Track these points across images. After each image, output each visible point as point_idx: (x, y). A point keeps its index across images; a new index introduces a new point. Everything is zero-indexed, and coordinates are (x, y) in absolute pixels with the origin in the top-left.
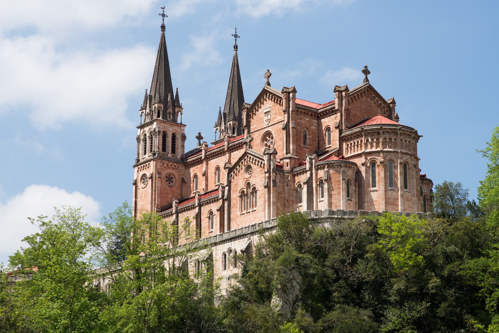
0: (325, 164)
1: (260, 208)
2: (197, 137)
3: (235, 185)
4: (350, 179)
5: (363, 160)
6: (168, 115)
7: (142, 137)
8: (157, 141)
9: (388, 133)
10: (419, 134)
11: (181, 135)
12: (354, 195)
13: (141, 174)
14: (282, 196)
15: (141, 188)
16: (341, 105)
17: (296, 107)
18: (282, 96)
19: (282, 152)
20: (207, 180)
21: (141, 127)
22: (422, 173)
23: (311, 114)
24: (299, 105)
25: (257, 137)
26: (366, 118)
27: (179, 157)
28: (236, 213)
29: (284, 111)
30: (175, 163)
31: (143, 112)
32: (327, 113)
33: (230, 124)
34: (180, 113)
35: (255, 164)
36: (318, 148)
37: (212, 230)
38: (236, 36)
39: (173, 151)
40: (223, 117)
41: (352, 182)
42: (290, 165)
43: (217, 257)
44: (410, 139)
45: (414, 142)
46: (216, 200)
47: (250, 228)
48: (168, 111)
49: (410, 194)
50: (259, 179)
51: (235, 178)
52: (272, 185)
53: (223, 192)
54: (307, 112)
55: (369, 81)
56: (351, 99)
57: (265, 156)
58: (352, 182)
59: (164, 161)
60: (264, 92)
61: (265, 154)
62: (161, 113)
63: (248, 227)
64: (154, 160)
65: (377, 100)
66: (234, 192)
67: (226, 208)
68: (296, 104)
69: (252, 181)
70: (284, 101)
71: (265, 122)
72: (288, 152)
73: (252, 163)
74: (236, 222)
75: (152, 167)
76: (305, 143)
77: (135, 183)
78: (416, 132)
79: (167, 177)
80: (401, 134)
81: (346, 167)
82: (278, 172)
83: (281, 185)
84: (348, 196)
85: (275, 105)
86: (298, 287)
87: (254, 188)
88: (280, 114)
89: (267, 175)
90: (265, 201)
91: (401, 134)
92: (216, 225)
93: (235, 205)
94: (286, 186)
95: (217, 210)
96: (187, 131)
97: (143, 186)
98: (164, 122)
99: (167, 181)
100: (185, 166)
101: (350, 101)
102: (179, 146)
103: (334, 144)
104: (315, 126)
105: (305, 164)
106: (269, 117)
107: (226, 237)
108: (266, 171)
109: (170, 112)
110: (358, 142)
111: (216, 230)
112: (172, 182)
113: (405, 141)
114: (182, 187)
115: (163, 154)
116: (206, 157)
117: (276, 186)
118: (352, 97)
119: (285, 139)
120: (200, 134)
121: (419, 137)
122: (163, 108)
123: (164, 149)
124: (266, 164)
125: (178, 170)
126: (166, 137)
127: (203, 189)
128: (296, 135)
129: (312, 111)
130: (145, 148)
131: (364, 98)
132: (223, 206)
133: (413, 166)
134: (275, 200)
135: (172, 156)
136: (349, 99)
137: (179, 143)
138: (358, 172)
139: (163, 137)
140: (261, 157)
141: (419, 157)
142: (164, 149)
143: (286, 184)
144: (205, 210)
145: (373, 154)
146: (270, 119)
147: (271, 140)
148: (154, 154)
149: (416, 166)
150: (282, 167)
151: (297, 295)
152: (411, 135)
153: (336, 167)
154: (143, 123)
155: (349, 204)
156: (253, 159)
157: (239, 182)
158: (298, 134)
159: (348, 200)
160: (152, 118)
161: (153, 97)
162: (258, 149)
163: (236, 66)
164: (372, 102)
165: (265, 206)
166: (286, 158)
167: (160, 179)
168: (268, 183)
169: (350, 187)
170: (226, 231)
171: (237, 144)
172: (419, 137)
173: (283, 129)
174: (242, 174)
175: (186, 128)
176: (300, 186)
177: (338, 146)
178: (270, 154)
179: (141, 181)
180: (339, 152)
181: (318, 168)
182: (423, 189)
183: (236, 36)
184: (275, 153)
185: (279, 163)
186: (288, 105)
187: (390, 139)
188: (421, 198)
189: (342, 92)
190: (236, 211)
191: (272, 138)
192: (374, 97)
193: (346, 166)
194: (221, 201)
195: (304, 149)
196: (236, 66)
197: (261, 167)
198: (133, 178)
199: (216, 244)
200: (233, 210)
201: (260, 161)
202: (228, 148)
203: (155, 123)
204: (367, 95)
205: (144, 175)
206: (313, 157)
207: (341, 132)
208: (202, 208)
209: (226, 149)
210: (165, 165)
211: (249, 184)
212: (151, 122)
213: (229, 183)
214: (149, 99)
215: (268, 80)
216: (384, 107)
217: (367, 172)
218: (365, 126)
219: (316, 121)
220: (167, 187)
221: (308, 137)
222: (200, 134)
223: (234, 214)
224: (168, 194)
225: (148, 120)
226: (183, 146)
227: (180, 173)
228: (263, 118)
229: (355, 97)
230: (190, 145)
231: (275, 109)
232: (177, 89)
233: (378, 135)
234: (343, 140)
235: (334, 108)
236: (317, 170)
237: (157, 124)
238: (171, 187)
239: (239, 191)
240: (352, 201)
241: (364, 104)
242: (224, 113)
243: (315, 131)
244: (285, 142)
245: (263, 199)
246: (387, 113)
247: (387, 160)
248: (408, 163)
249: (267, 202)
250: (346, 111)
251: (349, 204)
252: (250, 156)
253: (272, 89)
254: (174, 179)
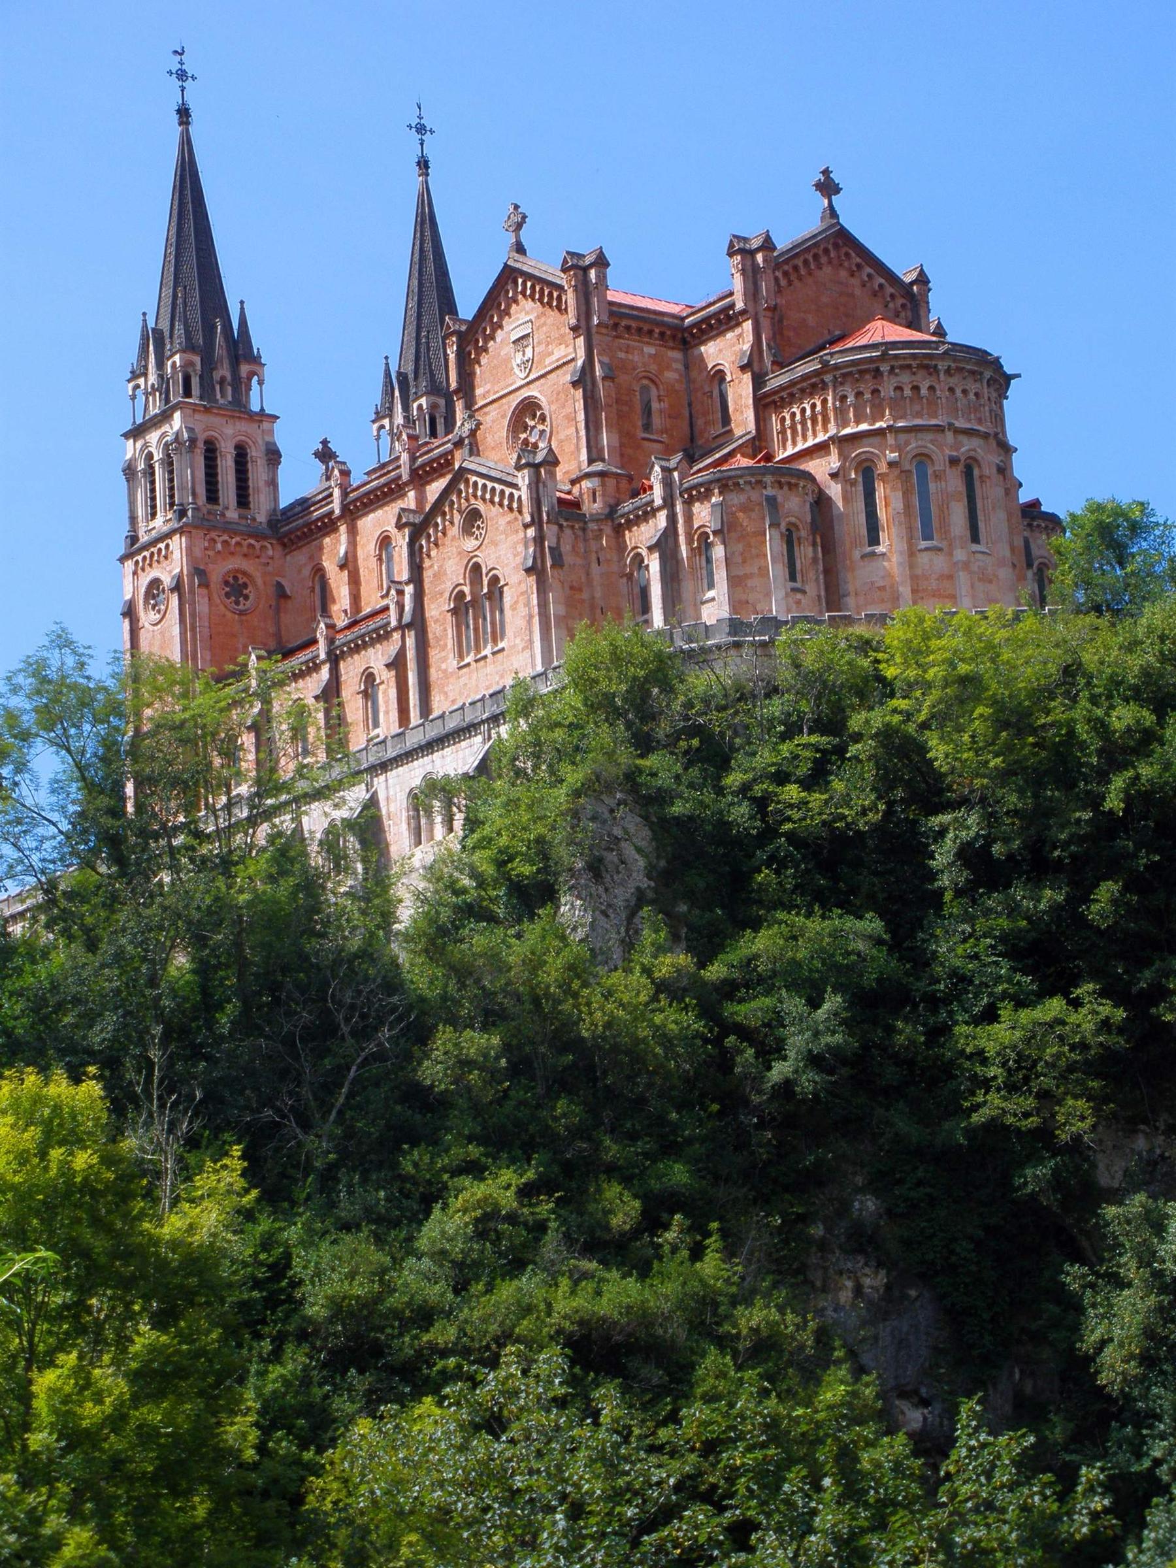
0: (711, 482)
1: (518, 641)
2: (317, 454)
3: (435, 575)
4: (794, 524)
5: (833, 461)
6: (218, 387)
7: (141, 466)
8: (191, 473)
9: (908, 372)
10: (1008, 370)
11: (263, 448)
12: (812, 575)
13: (144, 580)
14: (585, 596)
15: (147, 625)
16: (752, 292)
17: (612, 314)
18: (562, 279)
19: (573, 459)
20: (355, 581)
21: (137, 432)
22: (1024, 496)
23: (662, 334)
24: (620, 305)
25: (495, 424)
26: (837, 333)
27: (262, 518)
28: (444, 666)
29: (574, 329)
30: (251, 536)
31: (137, 386)
32: (711, 326)
33: (420, 407)
34: (255, 378)
35: (492, 502)
36: (692, 440)
37: (377, 731)
38: (421, 129)
39: (243, 500)
40: (400, 386)
41: (803, 533)
42: (603, 495)
43: (392, 809)
44: (978, 385)
45: (994, 395)
46: (382, 635)
47: (488, 702)
48: (217, 375)
49: (988, 559)
50: (506, 548)
51: (433, 553)
52: (549, 563)
53: (401, 607)
54: (646, 328)
55: (837, 217)
56: (786, 274)
57: (519, 474)
58: (803, 533)
59: (213, 535)
60: (508, 275)
61: (519, 468)
62: (195, 382)
63: (482, 699)
64: (180, 531)
65: (869, 276)
66: (434, 598)
67: (411, 654)
68: (611, 304)
69: (486, 559)
70: (570, 297)
71: (517, 370)
72: (594, 456)
73: (484, 499)
74: (446, 693)
75: (177, 555)
76: (647, 427)
77: (130, 612)
78: (996, 364)
79: (226, 583)
80: (948, 372)
81: (780, 485)
82: (566, 520)
83: (579, 561)
84: (793, 577)
85: (543, 314)
86: (642, 863)
87: (495, 580)
88: (561, 341)
89: (531, 532)
90: (531, 617)
91: (948, 372)
92: (387, 712)
93: (438, 639)
94: (594, 565)
95: (388, 666)
96: (282, 436)
97: (154, 616)
98: (207, 410)
99: (227, 595)
100: (284, 545)
101: (783, 283)
102: (261, 484)
103: (744, 421)
104: (676, 370)
105: (651, 488)
106: (529, 351)
107: (414, 739)
108: (528, 519)
109: (222, 381)
110: (813, 406)
111: (388, 724)
112: (246, 597)
113: (965, 392)
114: (278, 610)
115: (209, 513)
116: (344, 508)
117: (561, 566)
118: (786, 267)
119: (581, 416)
120: (325, 442)
121: (1008, 378)
122: (199, 367)
123: (212, 495)
124: (524, 498)
125: (263, 560)
127: (345, 611)
128: (618, 401)
129: (663, 324)
130: (153, 499)
131: (828, 270)
132: (401, 654)
133: (994, 470)
134: (562, 611)
135: (240, 517)
136: (779, 274)
137: (258, 473)
138: (821, 501)
139: (206, 458)
140: (509, 479)
141: (1012, 442)
142: (212, 495)
143: (594, 557)
144: (351, 670)
145: (865, 441)
146: (533, 357)
147: (541, 427)
148: (182, 514)
149: (1004, 470)
150: (576, 504)
151: (638, 889)
152: (981, 374)
153: (748, 488)
154: (139, 421)
155: (798, 602)
156: (485, 486)
157: (447, 567)
158: (624, 398)
159: (793, 590)
160: (167, 400)
161: (167, 334)
162: (497, 454)
163: (426, 222)
164: (855, 281)
165: (531, 632)
166: (588, 476)
167: (205, 591)
168: (535, 558)
169: (796, 548)
170: (415, 718)
171: (441, 456)
172: (1008, 378)
173: (575, 384)
174: (454, 538)
175: (277, 426)
176: (638, 559)
177: (752, 426)
178: (536, 467)
179: (146, 602)
180: (758, 444)
181: (691, 496)
182: (1033, 546)
183: (421, 129)
184: (552, 461)
185: (569, 493)
186: (583, 308)
187: (916, 388)
188: (1030, 574)
189: (752, 253)
190: (444, 659)
191: (543, 419)
192: (859, 266)
193: (779, 482)
194: (396, 636)
195: (646, 443)
196: (426, 222)
197: (511, 509)
198: (123, 596)
199: (384, 766)
200: (434, 655)
201: (508, 491)
202: (413, 472)
203: (177, 415)
204: (835, 262)
205: (155, 583)
206: (673, 463)
207: (758, 381)
208: (342, 665)
209: (405, 477)
210: (219, 546)
211: (477, 568)
212: (164, 412)
213: (417, 576)
214: (155, 341)
215: (518, 236)
216: (892, 296)
217: (846, 498)
218: (831, 354)
219: (677, 355)
220: (229, 615)
221: (655, 405)
222: (325, 442)
223: (439, 669)
224: (234, 636)
225: (154, 410)
226: (273, 483)
227: (270, 568)
228: (508, 360)
229: (796, 268)
230: (297, 480)
231: (544, 324)
232: (242, 302)
233: (875, 377)
234: (766, 406)
235: (732, 306)
236: (689, 503)
237: (183, 418)
238: (241, 613)
239: (447, 595)
240: (804, 592)
241: (823, 289)
242: (399, 374)
243: (677, 386)
244: (582, 425)
245: (523, 611)
246: (903, 314)
247: (910, 456)
248: (976, 460)
249: (536, 620)
250: (769, 314)
251: (798, 602)
252: (474, 478)
253: (527, 265)
254: (250, 588)
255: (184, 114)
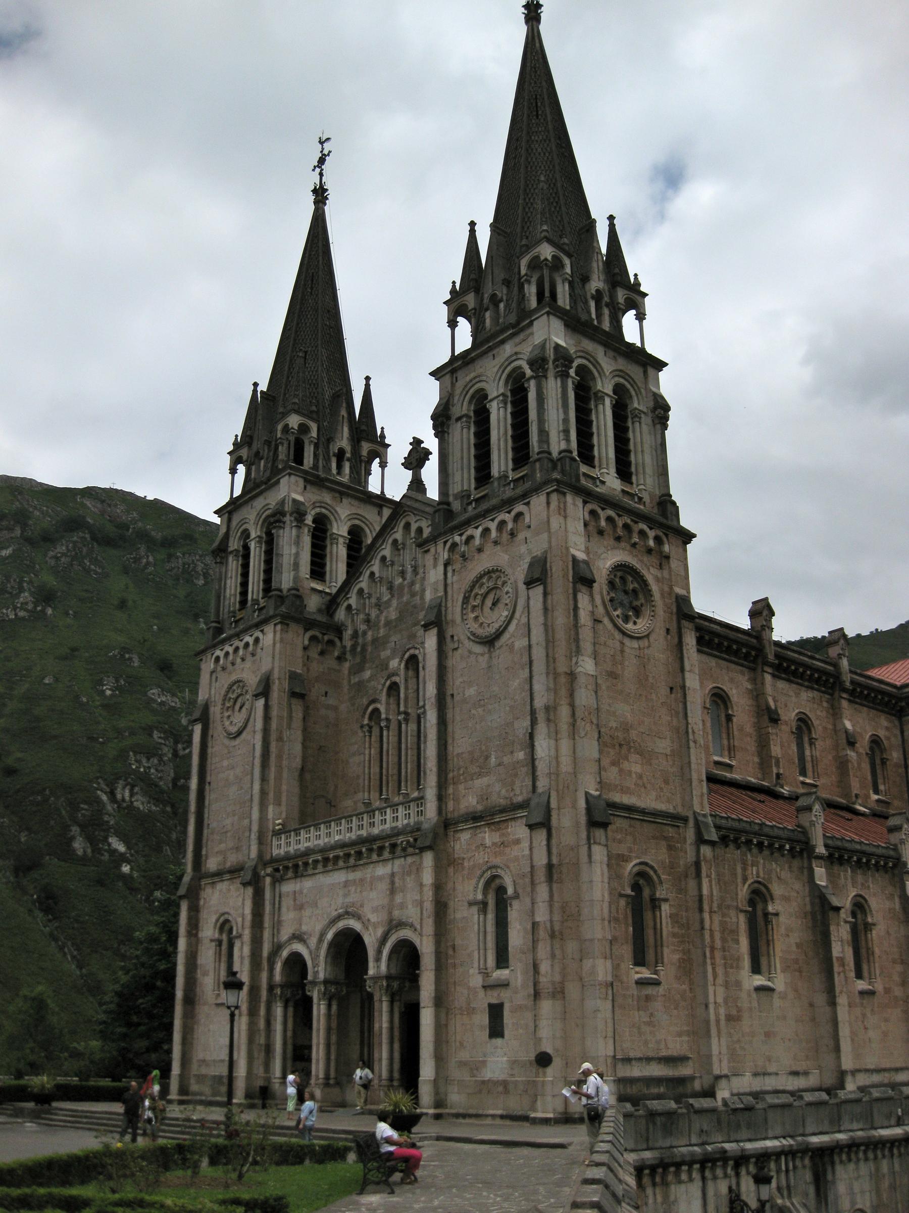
34: (377, 460)
48: (334, 448)
109: (341, 452)
122: (314, 434)
126: (325, 538)
203: (284, 481)
232: (368, 379)
255: (320, 194)
